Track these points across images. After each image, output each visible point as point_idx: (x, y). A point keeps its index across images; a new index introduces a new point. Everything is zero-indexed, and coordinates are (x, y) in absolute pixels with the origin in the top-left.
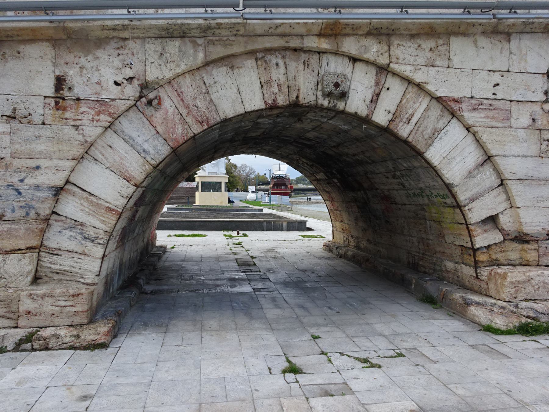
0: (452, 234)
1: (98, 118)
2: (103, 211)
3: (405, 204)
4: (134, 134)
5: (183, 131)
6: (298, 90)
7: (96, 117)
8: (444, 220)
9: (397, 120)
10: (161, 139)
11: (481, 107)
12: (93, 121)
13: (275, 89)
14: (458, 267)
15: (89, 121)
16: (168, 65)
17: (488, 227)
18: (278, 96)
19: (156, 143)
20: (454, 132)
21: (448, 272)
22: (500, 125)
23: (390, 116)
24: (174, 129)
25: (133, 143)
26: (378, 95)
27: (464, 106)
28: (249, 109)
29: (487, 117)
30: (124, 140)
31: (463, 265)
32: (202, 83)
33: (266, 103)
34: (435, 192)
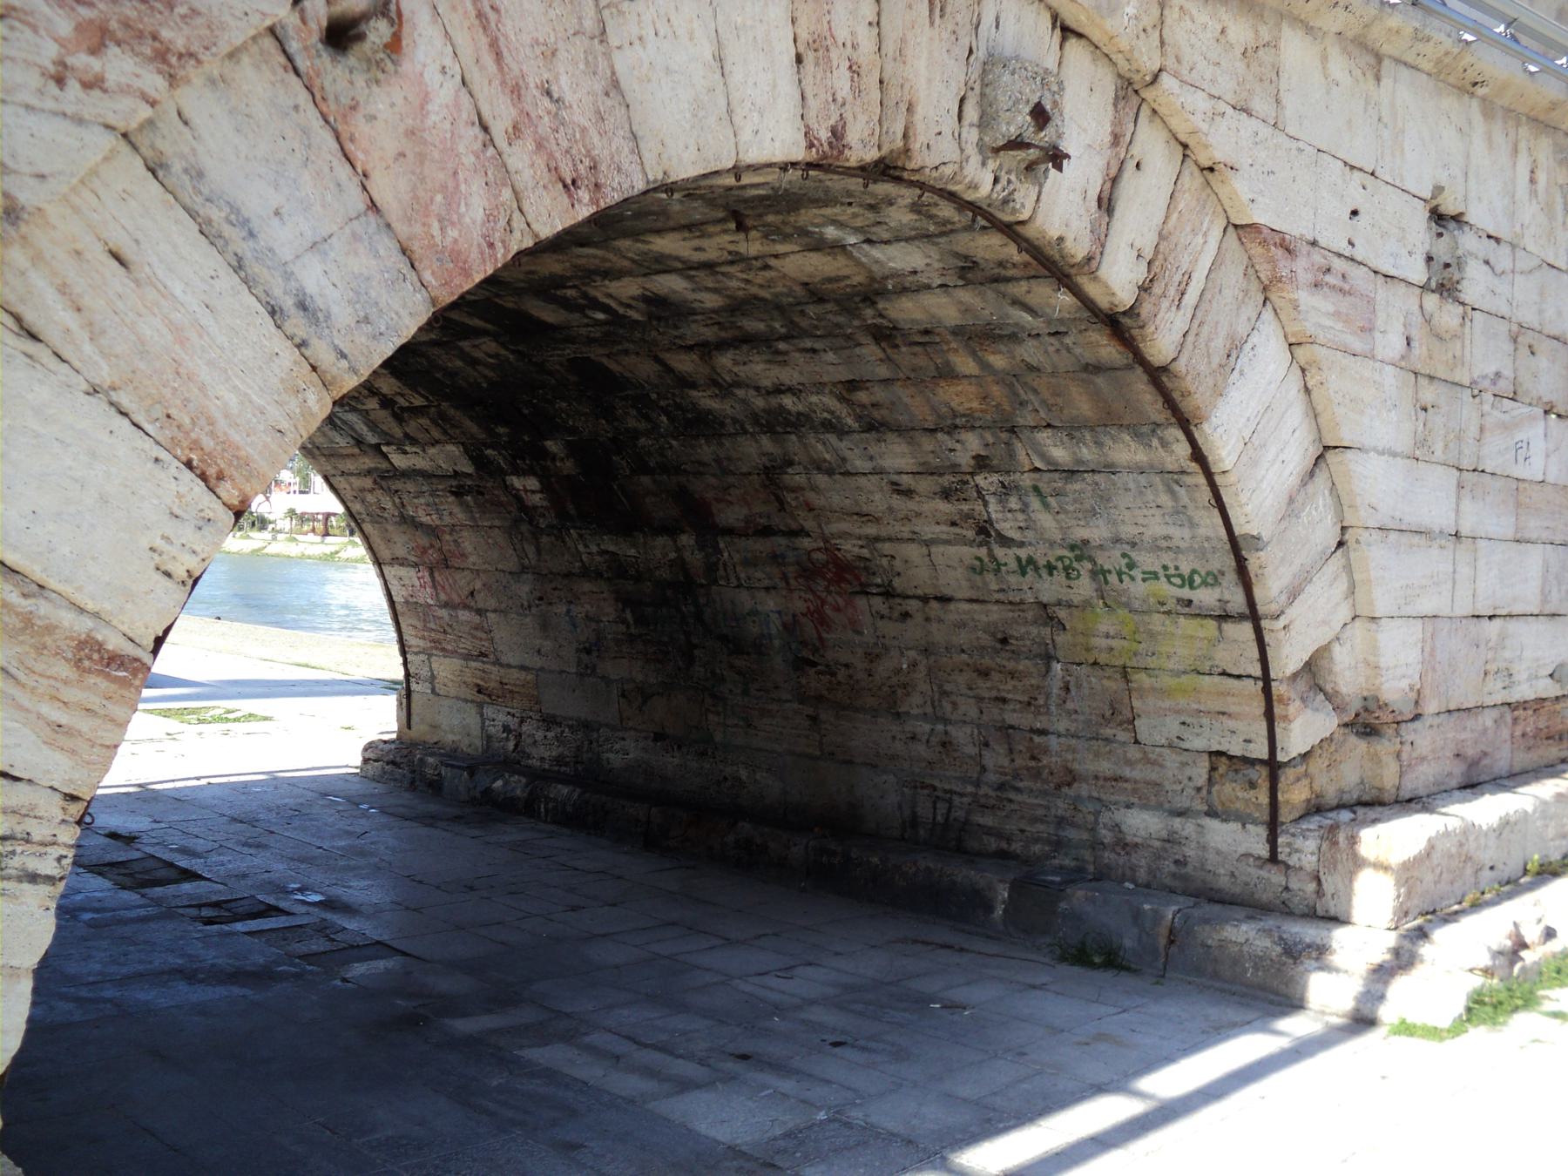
0: (1178, 712)
1: (95, 64)
2: (64, 670)
3: (945, 600)
4: (256, 199)
5: (489, 217)
6: (910, 109)
7: (81, 60)
8: (1152, 662)
10: (387, 247)
12: (60, 81)
13: (842, 82)
14: (1186, 827)
15: (35, 80)
18: (848, 116)
19: (362, 263)
20: (1267, 358)
21: (1124, 845)
23: (1141, 274)
24: (452, 196)
25: (246, 249)
27: (1302, 268)
28: (753, 156)
29: (1337, 314)
30: (206, 230)
31: (1213, 824)
34: (1147, 561)
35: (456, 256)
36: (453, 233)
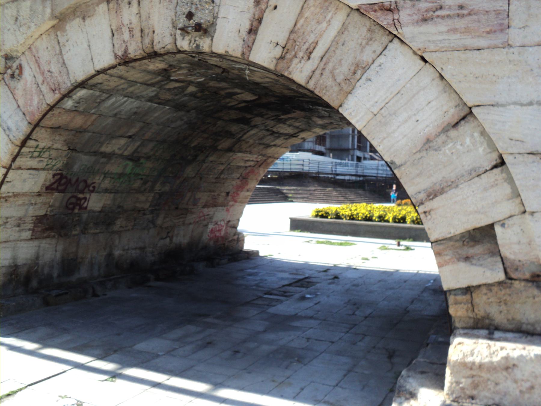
5: (38, 103)
9: (288, 56)
10: (21, 114)
11: (439, 13)
13: (126, 36)
16: (21, 29)
17: (478, 249)
18: (128, 44)
22: (482, 43)
23: (278, 52)
24: (31, 100)
26: (260, 21)
27: (404, 15)
29: (454, 30)
32: (56, 43)
33: (116, 56)
35: (32, 113)
36: (32, 108)
